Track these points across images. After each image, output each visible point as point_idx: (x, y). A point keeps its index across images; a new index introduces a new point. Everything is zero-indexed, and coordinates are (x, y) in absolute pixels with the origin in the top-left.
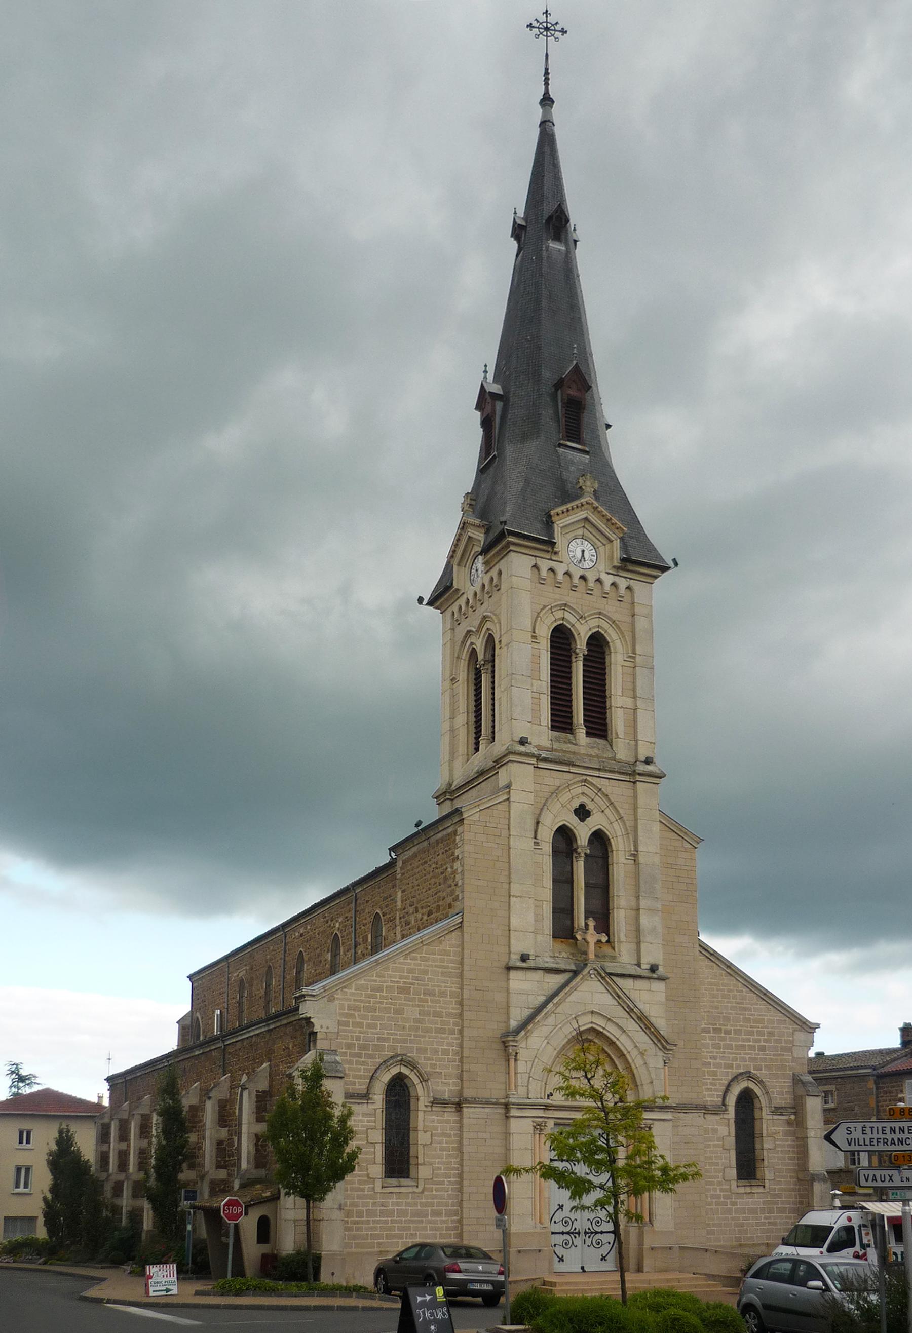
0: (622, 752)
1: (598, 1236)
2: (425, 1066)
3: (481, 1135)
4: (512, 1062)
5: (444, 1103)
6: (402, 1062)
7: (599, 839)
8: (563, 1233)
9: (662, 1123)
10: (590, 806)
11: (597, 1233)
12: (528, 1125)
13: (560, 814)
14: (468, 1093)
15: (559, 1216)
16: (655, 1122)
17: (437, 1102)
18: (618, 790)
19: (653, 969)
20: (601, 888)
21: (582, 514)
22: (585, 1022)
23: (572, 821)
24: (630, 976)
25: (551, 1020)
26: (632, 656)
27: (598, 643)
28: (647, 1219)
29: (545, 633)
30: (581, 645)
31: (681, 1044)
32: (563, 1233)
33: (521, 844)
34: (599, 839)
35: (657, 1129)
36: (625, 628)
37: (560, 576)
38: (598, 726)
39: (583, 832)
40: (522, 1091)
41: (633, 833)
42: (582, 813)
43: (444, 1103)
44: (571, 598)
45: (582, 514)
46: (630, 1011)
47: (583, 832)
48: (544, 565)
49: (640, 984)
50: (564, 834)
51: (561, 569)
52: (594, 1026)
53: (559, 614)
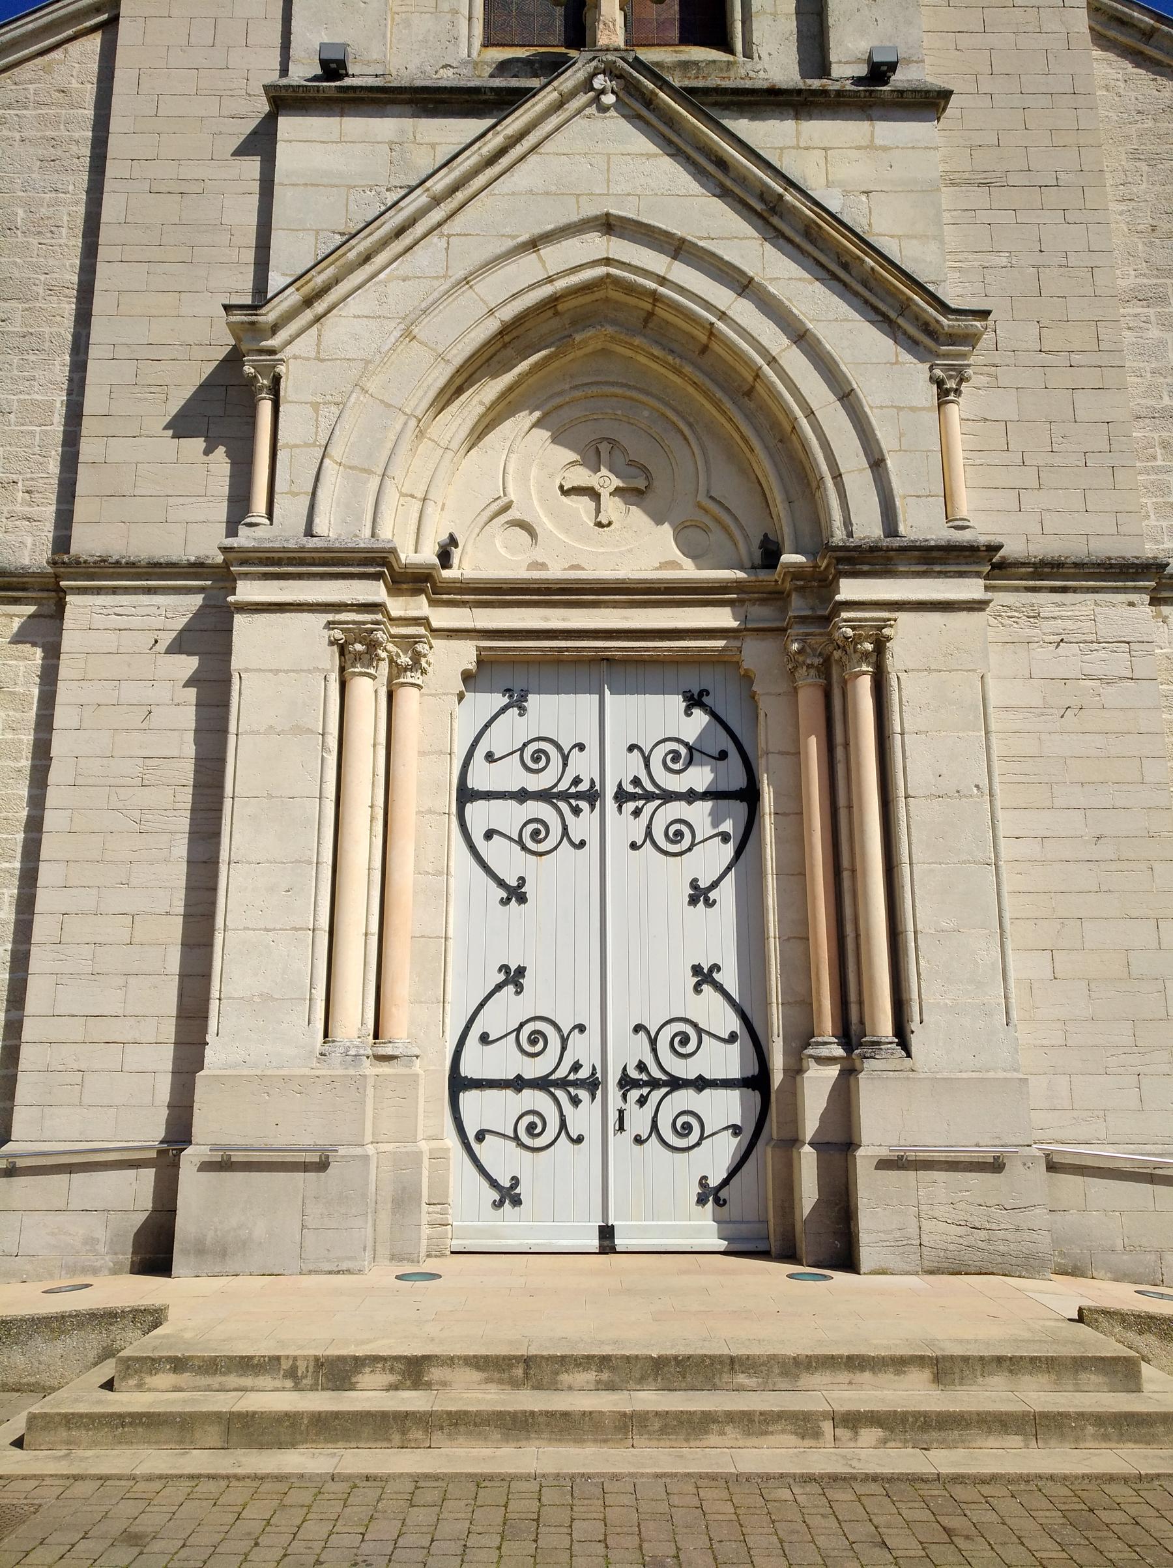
1: (684, 1099)
3: (130, 692)
4: (265, 408)
8: (518, 1084)
9: (936, 617)
11: (676, 1083)
14: (87, 541)
15: (505, 1012)
16: (903, 617)
19: (879, 72)
28: (885, 1027)
32: (518, 1084)
35: (909, 639)
40: (291, 510)
49: (820, 130)
52: (612, 271)
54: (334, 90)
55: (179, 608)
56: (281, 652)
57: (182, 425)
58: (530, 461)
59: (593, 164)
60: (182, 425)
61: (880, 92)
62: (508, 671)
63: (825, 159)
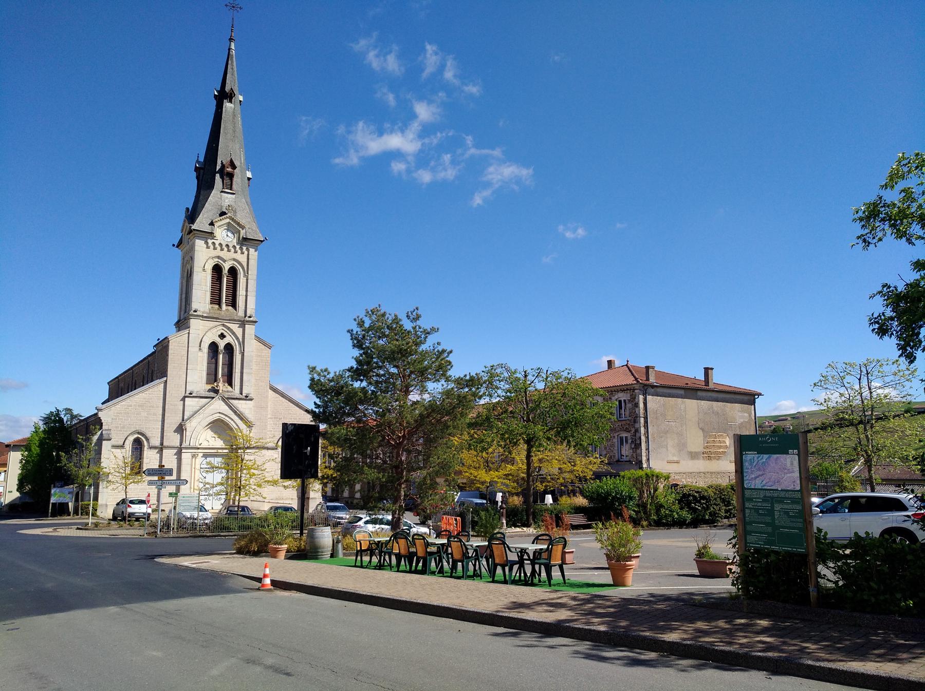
2: (148, 434)
5: (155, 448)
6: (139, 433)
7: (229, 347)
10: (225, 334)
12: (189, 455)
13: (212, 337)
17: (151, 448)
20: (230, 365)
21: (228, 220)
22: (216, 416)
23: (218, 340)
24: (237, 399)
25: (201, 416)
27: (233, 272)
29: (209, 267)
31: (258, 423)
33: (194, 349)
34: (229, 347)
36: (245, 265)
37: (217, 246)
39: (222, 344)
41: (242, 344)
43: (155, 448)
44: (222, 254)
45: (228, 220)
46: (235, 412)
47: (222, 344)
48: (210, 241)
50: (213, 347)
51: (217, 243)
54: (191, 395)
55: (175, 451)
56: (186, 456)
57: (175, 431)
58: (209, 434)
59: (218, 407)
60: (175, 431)
61: (247, 398)
62: (206, 456)
63: (241, 405)
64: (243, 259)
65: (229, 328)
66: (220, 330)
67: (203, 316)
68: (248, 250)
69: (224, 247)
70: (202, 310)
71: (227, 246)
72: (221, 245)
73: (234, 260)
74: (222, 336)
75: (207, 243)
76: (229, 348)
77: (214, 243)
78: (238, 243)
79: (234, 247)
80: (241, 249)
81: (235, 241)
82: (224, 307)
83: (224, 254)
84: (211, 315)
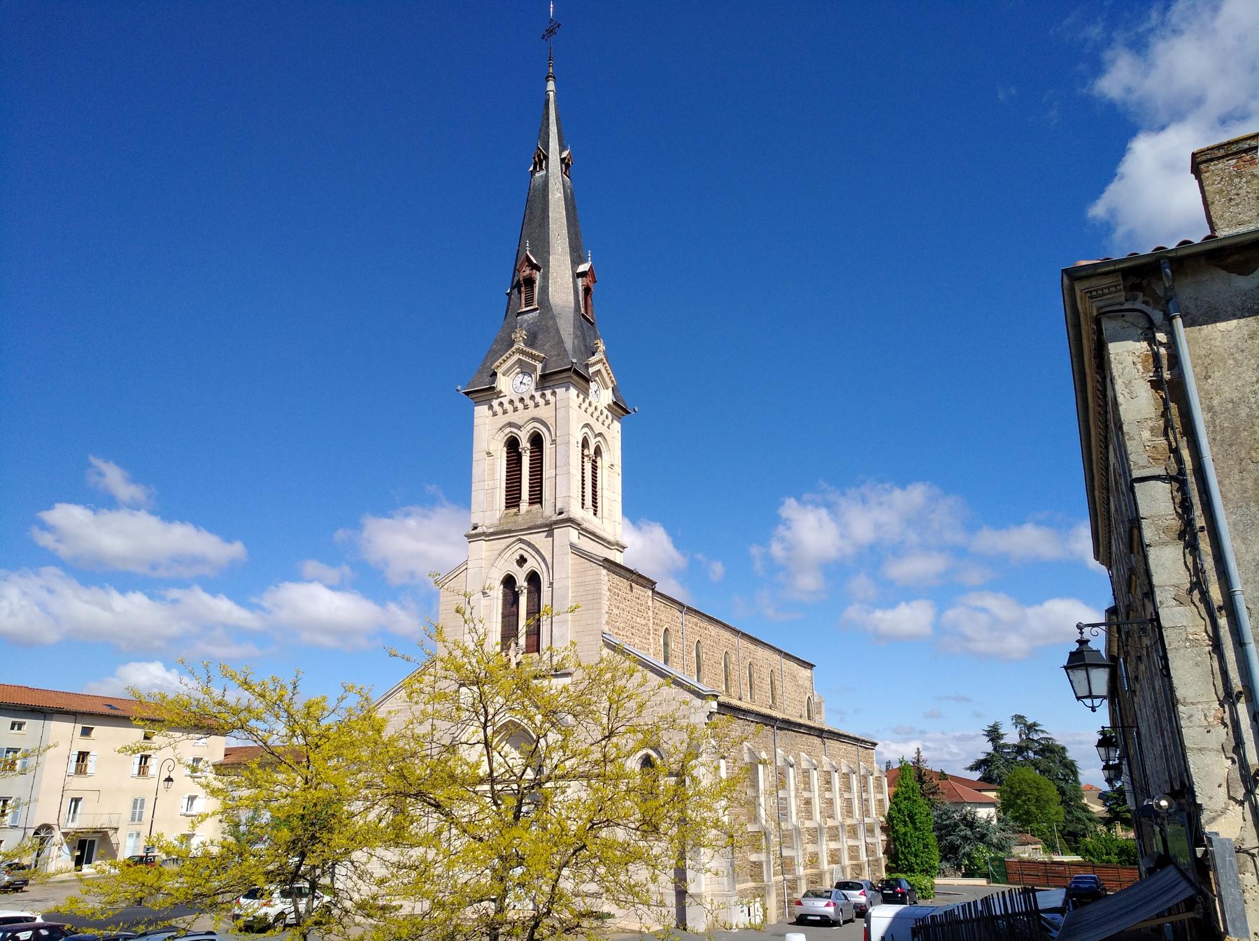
0: (548, 510)
18: (539, 539)
20: (535, 610)
21: (517, 357)
26: (554, 442)
30: (525, 444)
37: (506, 405)
38: (537, 498)
41: (550, 569)
42: (522, 561)
45: (517, 357)
48: (495, 403)
50: (509, 581)
51: (505, 401)
53: (509, 430)
64: (544, 412)
65: (529, 544)
66: (517, 550)
67: (484, 534)
68: (554, 393)
69: (517, 404)
70: (487, 523)
71: (522, 400)
72: (511, 402)
73: (535, 419)
74: (522, 561)
75: (491, 407)
76: (533, 578)
77: (501, 404)
78: (537, 389)
79: (532, 397)
80: (543, 395)
81: (533, 386)
82: (524, 506)
83: (520, 417)
84: (500, 528)
